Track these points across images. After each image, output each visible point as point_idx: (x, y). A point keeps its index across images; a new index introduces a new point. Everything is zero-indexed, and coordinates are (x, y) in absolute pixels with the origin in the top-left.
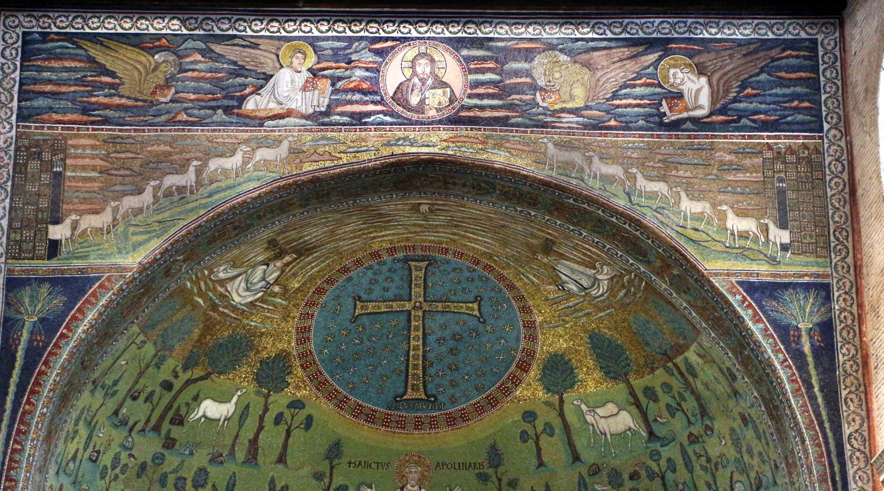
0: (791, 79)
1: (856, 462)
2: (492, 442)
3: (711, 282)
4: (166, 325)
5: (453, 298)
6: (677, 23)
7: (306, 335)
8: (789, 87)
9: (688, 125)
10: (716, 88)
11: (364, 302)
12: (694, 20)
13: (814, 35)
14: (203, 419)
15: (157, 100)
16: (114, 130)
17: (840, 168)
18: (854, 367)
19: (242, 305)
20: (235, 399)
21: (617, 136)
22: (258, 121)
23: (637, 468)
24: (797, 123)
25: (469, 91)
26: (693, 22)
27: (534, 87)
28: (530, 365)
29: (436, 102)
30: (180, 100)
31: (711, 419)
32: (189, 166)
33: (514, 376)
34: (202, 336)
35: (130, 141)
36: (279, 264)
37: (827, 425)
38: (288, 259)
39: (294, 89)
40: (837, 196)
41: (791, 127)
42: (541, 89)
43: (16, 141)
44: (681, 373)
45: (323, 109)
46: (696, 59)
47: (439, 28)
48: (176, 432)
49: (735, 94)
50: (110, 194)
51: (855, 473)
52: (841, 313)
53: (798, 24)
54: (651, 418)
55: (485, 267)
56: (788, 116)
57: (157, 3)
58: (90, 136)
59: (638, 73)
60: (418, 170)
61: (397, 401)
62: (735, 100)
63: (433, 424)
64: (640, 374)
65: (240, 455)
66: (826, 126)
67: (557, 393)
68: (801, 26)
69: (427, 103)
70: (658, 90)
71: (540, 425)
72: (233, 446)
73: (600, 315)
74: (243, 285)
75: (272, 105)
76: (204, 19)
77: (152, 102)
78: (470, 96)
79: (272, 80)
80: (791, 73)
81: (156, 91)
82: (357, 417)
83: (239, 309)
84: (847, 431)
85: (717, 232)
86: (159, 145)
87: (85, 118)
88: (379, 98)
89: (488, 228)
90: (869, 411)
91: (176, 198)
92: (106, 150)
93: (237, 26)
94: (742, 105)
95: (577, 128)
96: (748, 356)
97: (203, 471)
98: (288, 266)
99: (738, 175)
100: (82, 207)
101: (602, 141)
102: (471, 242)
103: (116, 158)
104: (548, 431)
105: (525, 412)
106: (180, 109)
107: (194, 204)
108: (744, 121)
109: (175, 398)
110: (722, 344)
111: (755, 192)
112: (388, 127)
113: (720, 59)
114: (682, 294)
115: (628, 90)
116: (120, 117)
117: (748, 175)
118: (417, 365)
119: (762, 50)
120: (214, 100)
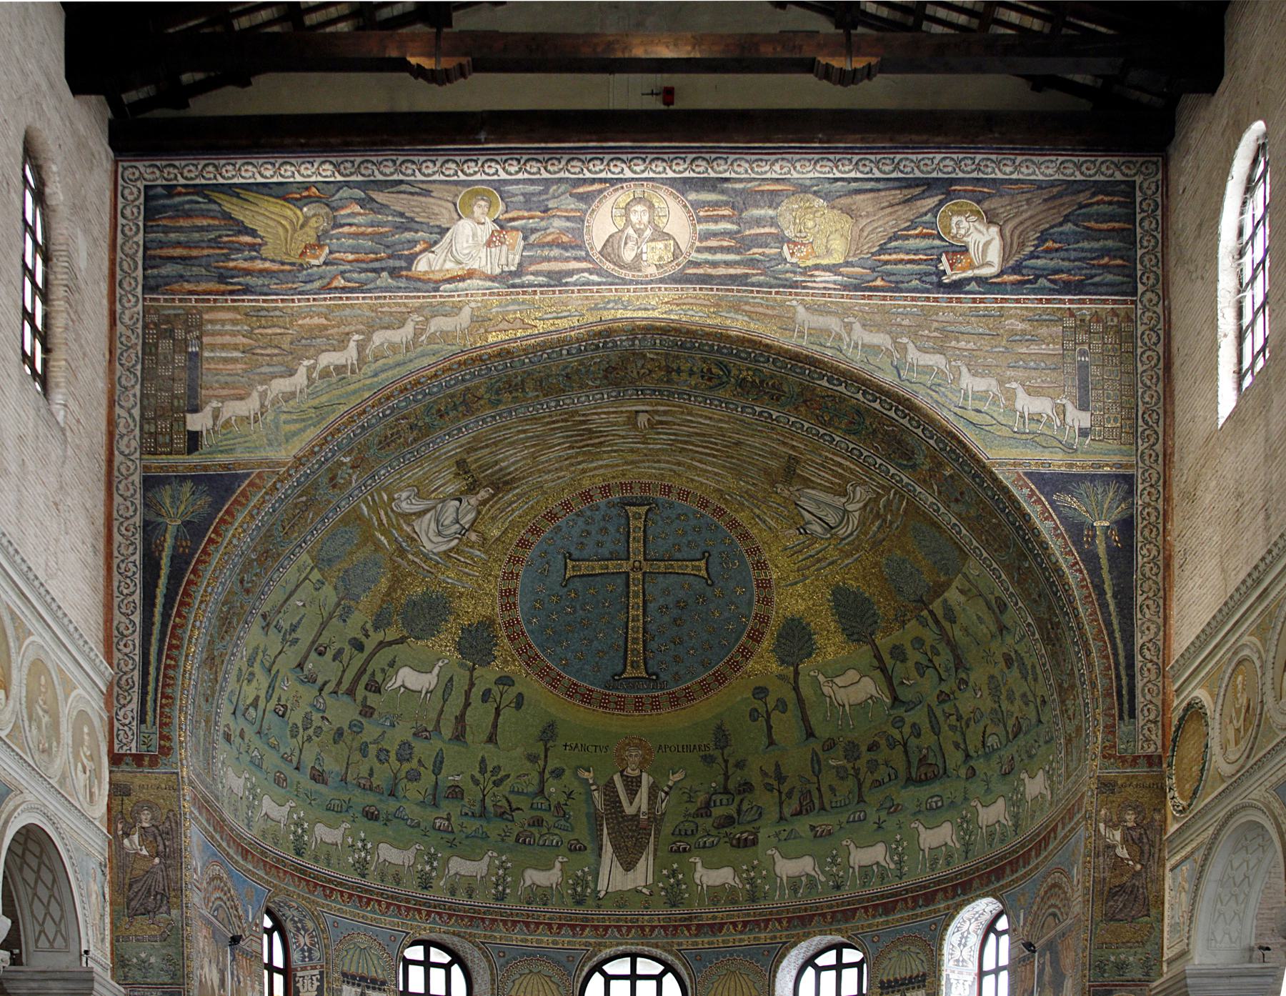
0: (1100, 230)
1: (1146, 674)
2: (719, 722)
3: (994, 473)
4: (346, 566)
5: (678, 555)
6: (963, 159)
7: (511, 600)
8: (1098, 240)
9: (973, 285)
10: (1009, 240)
11: (575, 560)
12: (985, 156)
13: (1131, 176)
14: (402, 689)
15: (308, 263)
16: (257, 301)
17: (1154, 339)
18: (1155, 570)
19: (434, 554)
20: (436, 670)
21: (884, 298)
22: (432, 285)
23: (876, 738)
24: (1106, 285)
25: (698, 244)
26: (983, 159)
27: (781, 239)
28: (763, 634)
29: (656, 257)
31: (967, 670)
32: (349, 341)
33: (745, 648)
34: (391, 589)
35: (277, 313)
36: (473, 501)
37: (1117, 635)
38: (483, 494)
39: (476, 245)
40: (1149, 373)
41: (1098, 288)
42: (789, 241)
43: (144, 316)
44: (937, 622)
45: (513, 268)
46: (986, 205)
47: (660, 166)
48: (373, 699)
49: (1032, 249)
50: (257, 377)
51: (1145, 685)
52: (1144, 509)
53: (1112, 163)
54: (895, 682)
55: (715, 510)
56: (1095, 275)
57: (303, 141)
58: (229, 309)
59: (912, 221)
60: (633, 345)
61: (616, 680)
62: (1032, 256)
63: (656, 705)
64: (887, 631)
65: (447, 732)
66: (1141, 288)
67: (793, 664)
68: (1116, 166)
69: (644, 258)
70: (937, 242)
71: (771, 703)
72: (438, 722)
73: (846, 562)
74: (433, 525)
75: (449, 265)
76: (362, 163)
77: (301, 265)
78: (699, 250)
79: (448, 234)
80: (1101, 223)
82: (572, 697)
83: (431, 559)
84: (1139, 640)
85: (1004, 414)
86: (312, 317)
87: (223, 287)
88: (583, 253)
89: (717, 450)
90: (1166, 619)
91: (334, 379)
92: (249, 325)
93: (403, 170)
94: (1040, 262)
95: (835, 289)
96: (1030, 568)
97: (405, 745)
98: (485, 506)
99: (1032, 347)
100: (225, 392)
101: (866, 305)
102: (698, 475)
103: (262, 335)
104: (781, 708)
105: (756, 688)
106: (335, 273)
107: (357, 385)
108: (1043, 282)
109: (368, 661)
110: (995, 565)
111: (1053, 366)
112: (595, 288)
113: (1014, 205)
114: (952, 505)
115: (900, 242)
116: (264, 285)
117: (1044, 347)
118: (637, 639)
119: (1067, 195)
120: (377, 260)
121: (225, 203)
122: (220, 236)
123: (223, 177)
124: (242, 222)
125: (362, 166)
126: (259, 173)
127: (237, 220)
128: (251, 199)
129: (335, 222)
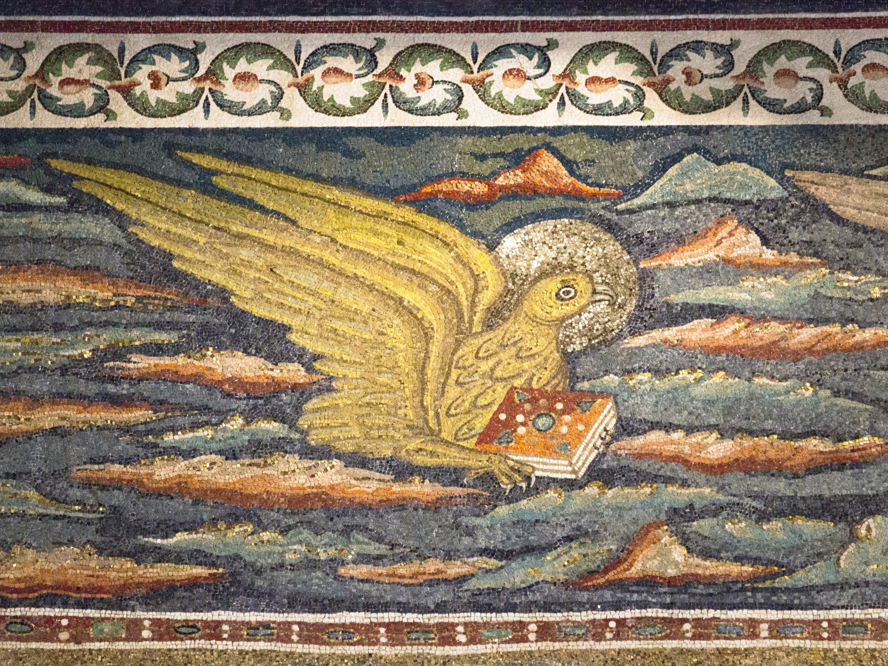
16: (283, 633)
30: (644, 465)
77: (488, 479)
81: (510, 424)
106: (648, 517)
116: (312, 564)
120: (837, 464)
121: (144, 214)
122: (118, 352)
123: (141, 106)
124: (223, 294)
125: (769, 70)
126: (303, 89)
127: (196, 284)
128: (260, 199)
129: (643, 299)
